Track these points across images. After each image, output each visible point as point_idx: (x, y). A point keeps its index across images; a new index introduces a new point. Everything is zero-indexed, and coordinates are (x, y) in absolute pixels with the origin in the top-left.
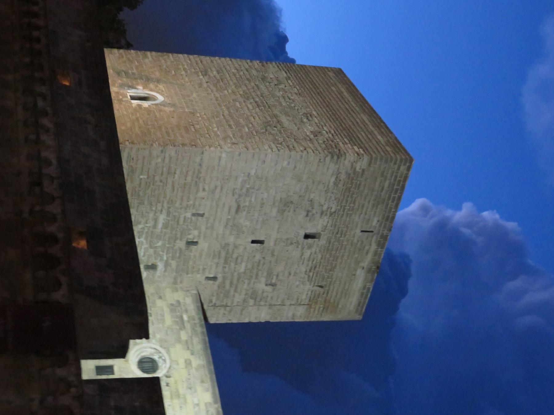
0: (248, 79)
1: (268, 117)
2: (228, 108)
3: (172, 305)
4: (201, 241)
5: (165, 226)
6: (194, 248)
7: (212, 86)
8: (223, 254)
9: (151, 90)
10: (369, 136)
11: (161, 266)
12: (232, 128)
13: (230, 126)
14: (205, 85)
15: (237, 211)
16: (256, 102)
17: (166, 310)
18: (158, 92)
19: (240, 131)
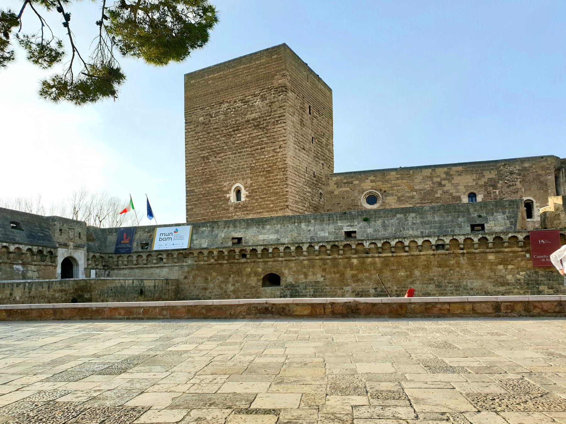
0: (209, 133)
1: (250, 126)
2: (243, 148)
3: (337, 187)
4: (314, 170)
5: (310, 187)
6: (316, 174)
7: (220, 156)
8: (317, 159)
9: (230, 189)
10: (262, 67)
11: (320, 191)
12: (264, 148)
13: (262, 148)
14: (220, 159)
15: (305, 150)
16: (234, 131)
17: (340, 190)
18: (232, 186)
19: (266, 143)
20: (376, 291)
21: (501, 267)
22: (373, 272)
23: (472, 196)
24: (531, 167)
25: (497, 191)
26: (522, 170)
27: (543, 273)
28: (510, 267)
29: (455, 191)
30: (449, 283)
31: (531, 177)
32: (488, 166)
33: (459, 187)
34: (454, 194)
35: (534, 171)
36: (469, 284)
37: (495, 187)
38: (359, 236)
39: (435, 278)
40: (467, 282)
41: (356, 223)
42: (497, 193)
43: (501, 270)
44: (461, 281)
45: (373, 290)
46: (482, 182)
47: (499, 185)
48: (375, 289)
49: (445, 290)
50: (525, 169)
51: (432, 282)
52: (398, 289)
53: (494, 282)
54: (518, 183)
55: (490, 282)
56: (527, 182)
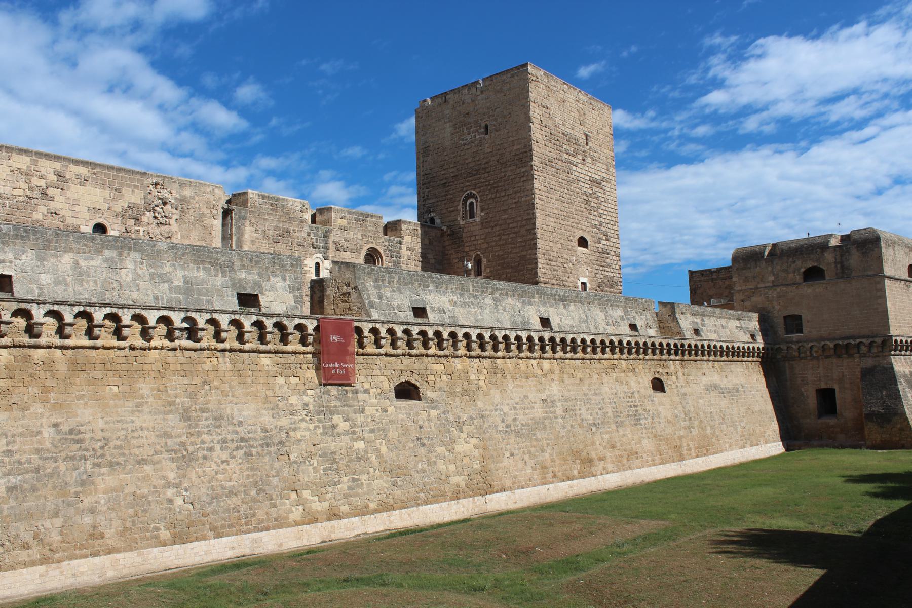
20: (58, 432)
21: (281, 380)
22: (50, 383)
23: (100, 228)
24: (194, 198)
25: (142, 229)
26: (181, 200)
27: (336, 393)
28: (294, 380)
29: (70, 214)
30: (203, 411)
31: (191, 215)
32: (131, 180)
33: (77, 208)
34: (69, 220)
35: (197, 206)
36: (236, 413)
37: (137, 220)
38: (19, 289)
39: (178, 401)
40: (232, 409)
41: (10, 256)
42: (141, 233)
43: (281, 387)
44: (223, 406)
45: (52, 430)
46: (118, 207)
47: (145, 219)
48: (55, 425)
49: (197, 425)
50: (183, 200)
51: (173, 408)
52: (107, 426)
53: (273, 409)
54: (173, 222)
55: (267, 409)
56: (186, 223)
